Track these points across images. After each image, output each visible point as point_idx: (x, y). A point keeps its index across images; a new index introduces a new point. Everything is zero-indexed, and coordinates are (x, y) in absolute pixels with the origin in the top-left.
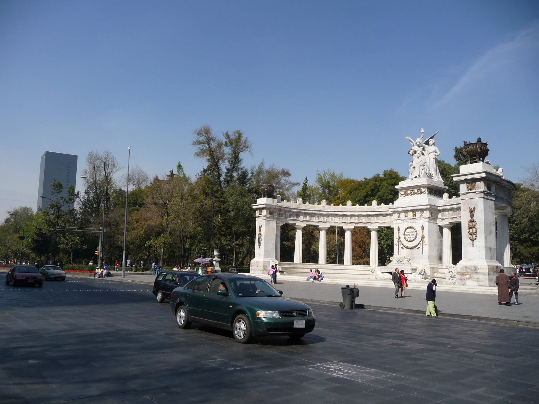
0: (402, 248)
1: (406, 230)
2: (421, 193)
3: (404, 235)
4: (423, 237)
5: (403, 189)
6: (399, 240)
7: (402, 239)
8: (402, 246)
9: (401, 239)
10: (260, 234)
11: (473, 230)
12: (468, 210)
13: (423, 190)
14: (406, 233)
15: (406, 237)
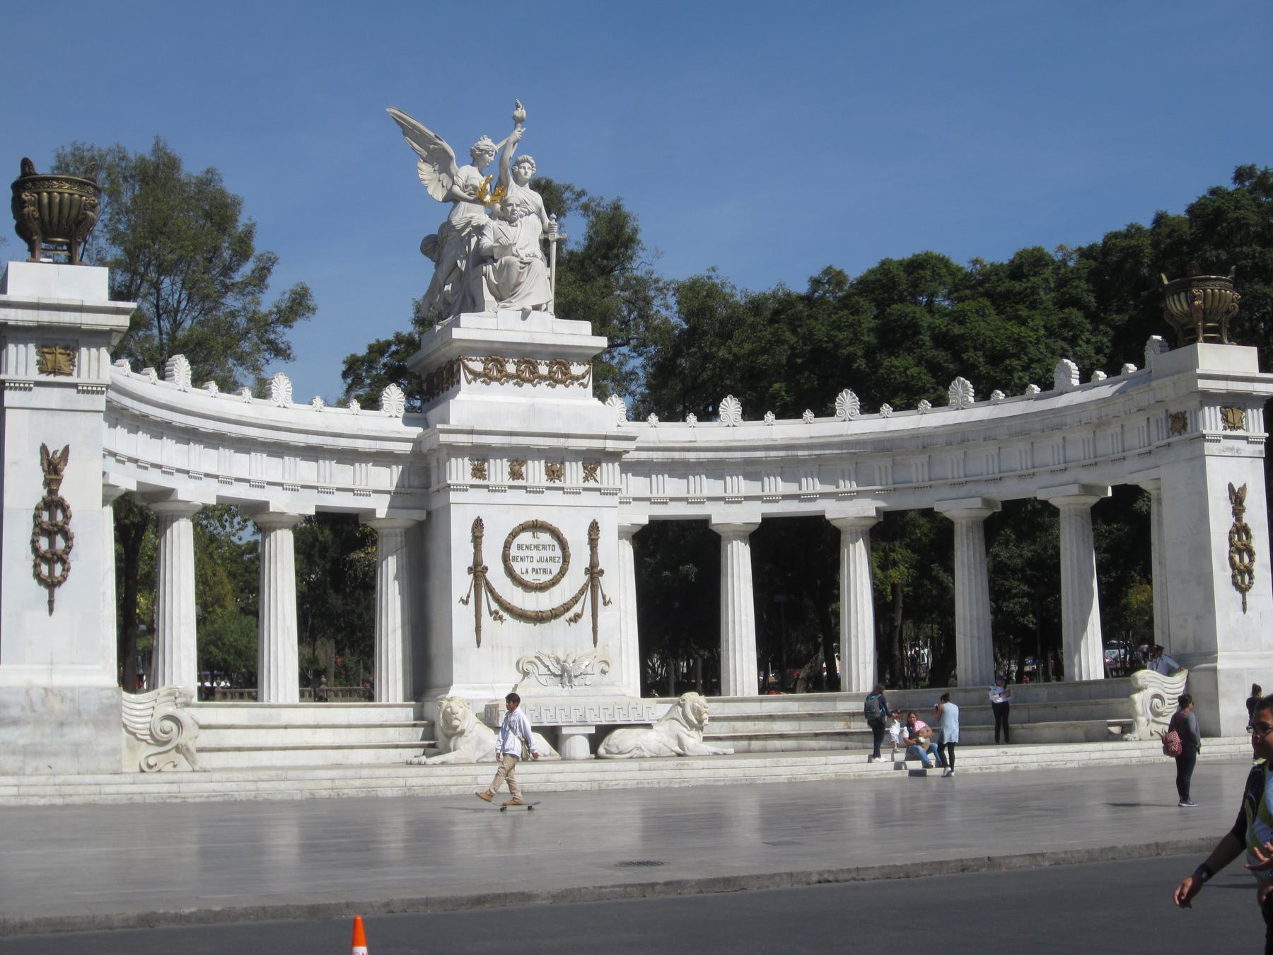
0: (496, 616)
1: (514, 535)
2: (568, 379)
3: (506, 558)
4: (594, 572)
5: (474, 349)
6: (476, 578)
7: (496, 574)
8: (495, 606)
9: (488, 575)
10: (53, 503)
11: (1241, 560)
12: (1227, 494)
13: (577, 369)
14: (513, 551)
15: (517, 567)
